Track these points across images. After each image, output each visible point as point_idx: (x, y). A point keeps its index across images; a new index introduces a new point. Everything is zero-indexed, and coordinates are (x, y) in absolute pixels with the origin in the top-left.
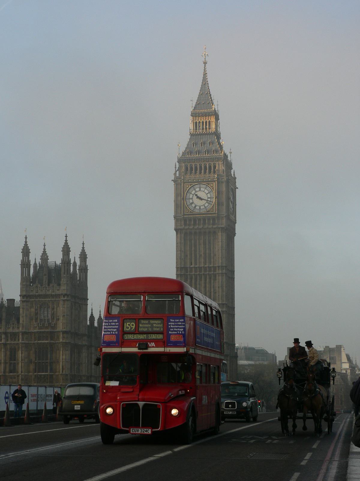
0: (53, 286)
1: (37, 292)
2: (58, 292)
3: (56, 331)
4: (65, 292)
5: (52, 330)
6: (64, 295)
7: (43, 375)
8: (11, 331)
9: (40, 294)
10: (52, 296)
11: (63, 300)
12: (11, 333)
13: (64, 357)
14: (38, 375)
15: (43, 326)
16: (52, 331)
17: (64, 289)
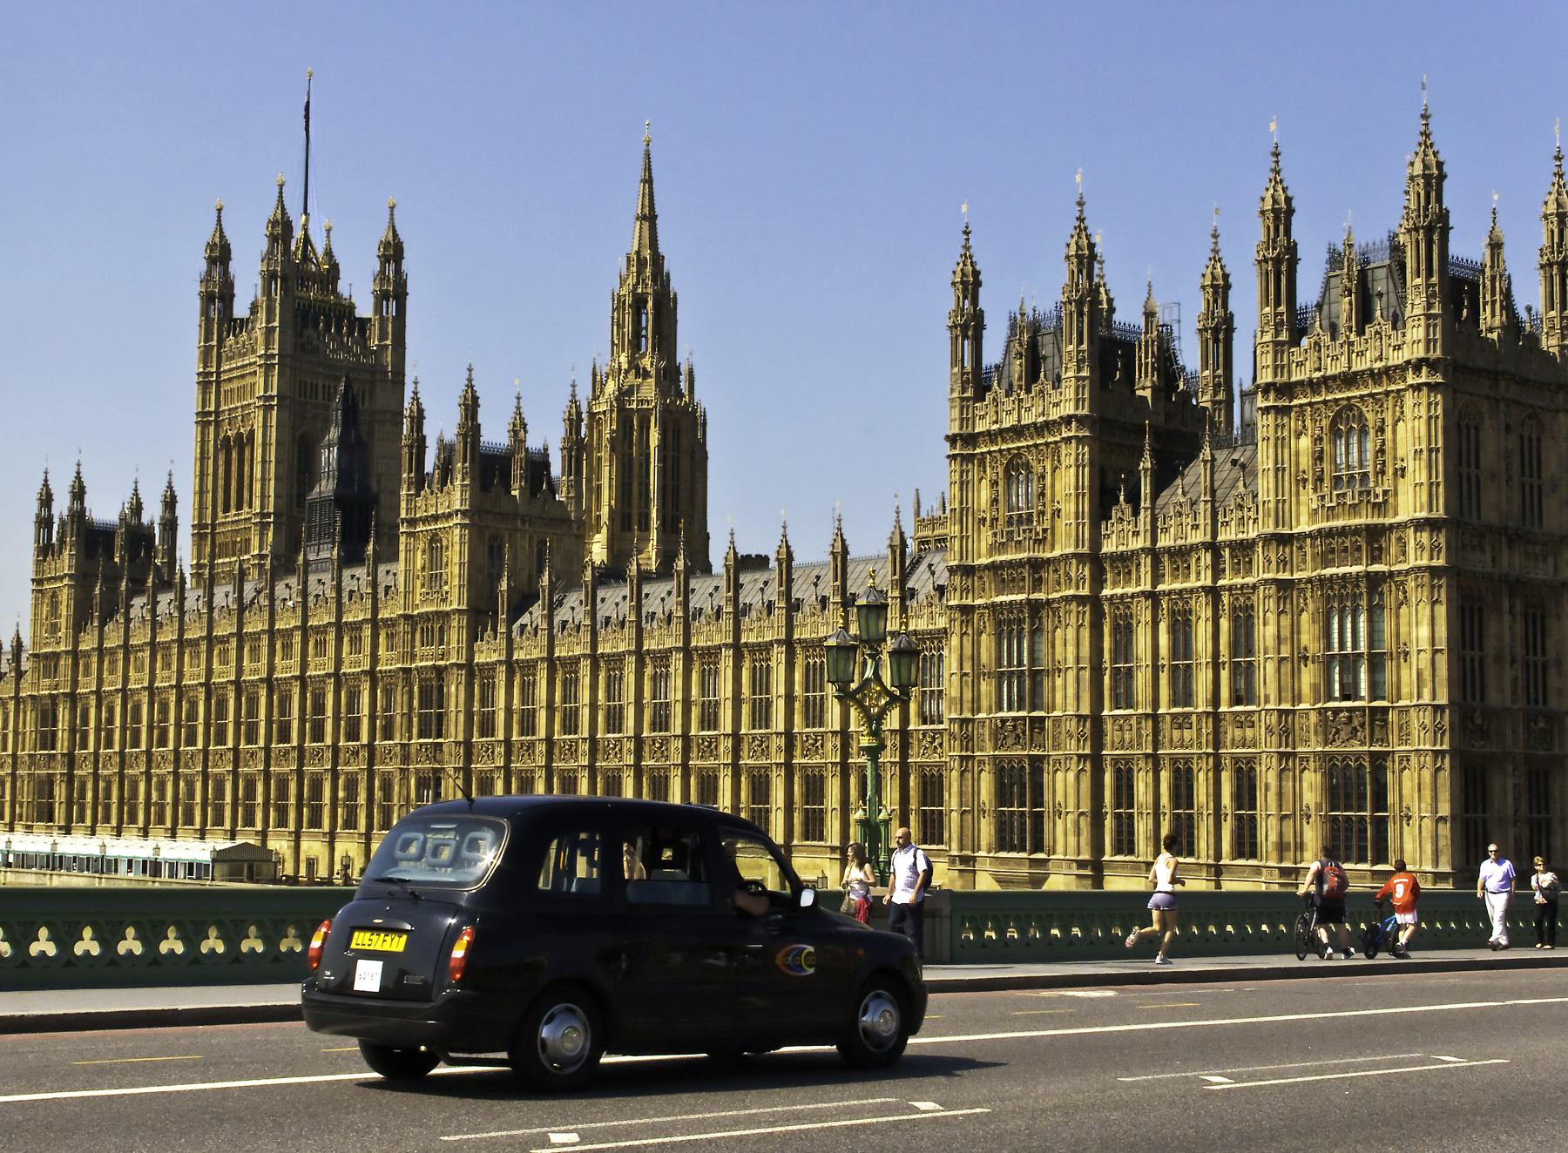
0: (1377, 333)
1: (1317, 366)
2: (1396, 359)
3: (1393, 521)
4: (1420, 352)
5: (1376, 520)
6: (1417, 366)
7: (1349, 710)
8: (1233, 537)
9: (1329, 373)
10: (1375, 376)
11: (1411, 386)
12: (1231, 541)
13: (1424, 632)
14: (1327, 710)
15: (1339, 504)
16: (1376, 525)
17: (1414, 341)
